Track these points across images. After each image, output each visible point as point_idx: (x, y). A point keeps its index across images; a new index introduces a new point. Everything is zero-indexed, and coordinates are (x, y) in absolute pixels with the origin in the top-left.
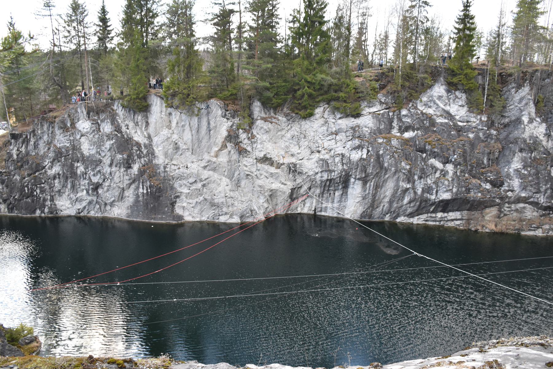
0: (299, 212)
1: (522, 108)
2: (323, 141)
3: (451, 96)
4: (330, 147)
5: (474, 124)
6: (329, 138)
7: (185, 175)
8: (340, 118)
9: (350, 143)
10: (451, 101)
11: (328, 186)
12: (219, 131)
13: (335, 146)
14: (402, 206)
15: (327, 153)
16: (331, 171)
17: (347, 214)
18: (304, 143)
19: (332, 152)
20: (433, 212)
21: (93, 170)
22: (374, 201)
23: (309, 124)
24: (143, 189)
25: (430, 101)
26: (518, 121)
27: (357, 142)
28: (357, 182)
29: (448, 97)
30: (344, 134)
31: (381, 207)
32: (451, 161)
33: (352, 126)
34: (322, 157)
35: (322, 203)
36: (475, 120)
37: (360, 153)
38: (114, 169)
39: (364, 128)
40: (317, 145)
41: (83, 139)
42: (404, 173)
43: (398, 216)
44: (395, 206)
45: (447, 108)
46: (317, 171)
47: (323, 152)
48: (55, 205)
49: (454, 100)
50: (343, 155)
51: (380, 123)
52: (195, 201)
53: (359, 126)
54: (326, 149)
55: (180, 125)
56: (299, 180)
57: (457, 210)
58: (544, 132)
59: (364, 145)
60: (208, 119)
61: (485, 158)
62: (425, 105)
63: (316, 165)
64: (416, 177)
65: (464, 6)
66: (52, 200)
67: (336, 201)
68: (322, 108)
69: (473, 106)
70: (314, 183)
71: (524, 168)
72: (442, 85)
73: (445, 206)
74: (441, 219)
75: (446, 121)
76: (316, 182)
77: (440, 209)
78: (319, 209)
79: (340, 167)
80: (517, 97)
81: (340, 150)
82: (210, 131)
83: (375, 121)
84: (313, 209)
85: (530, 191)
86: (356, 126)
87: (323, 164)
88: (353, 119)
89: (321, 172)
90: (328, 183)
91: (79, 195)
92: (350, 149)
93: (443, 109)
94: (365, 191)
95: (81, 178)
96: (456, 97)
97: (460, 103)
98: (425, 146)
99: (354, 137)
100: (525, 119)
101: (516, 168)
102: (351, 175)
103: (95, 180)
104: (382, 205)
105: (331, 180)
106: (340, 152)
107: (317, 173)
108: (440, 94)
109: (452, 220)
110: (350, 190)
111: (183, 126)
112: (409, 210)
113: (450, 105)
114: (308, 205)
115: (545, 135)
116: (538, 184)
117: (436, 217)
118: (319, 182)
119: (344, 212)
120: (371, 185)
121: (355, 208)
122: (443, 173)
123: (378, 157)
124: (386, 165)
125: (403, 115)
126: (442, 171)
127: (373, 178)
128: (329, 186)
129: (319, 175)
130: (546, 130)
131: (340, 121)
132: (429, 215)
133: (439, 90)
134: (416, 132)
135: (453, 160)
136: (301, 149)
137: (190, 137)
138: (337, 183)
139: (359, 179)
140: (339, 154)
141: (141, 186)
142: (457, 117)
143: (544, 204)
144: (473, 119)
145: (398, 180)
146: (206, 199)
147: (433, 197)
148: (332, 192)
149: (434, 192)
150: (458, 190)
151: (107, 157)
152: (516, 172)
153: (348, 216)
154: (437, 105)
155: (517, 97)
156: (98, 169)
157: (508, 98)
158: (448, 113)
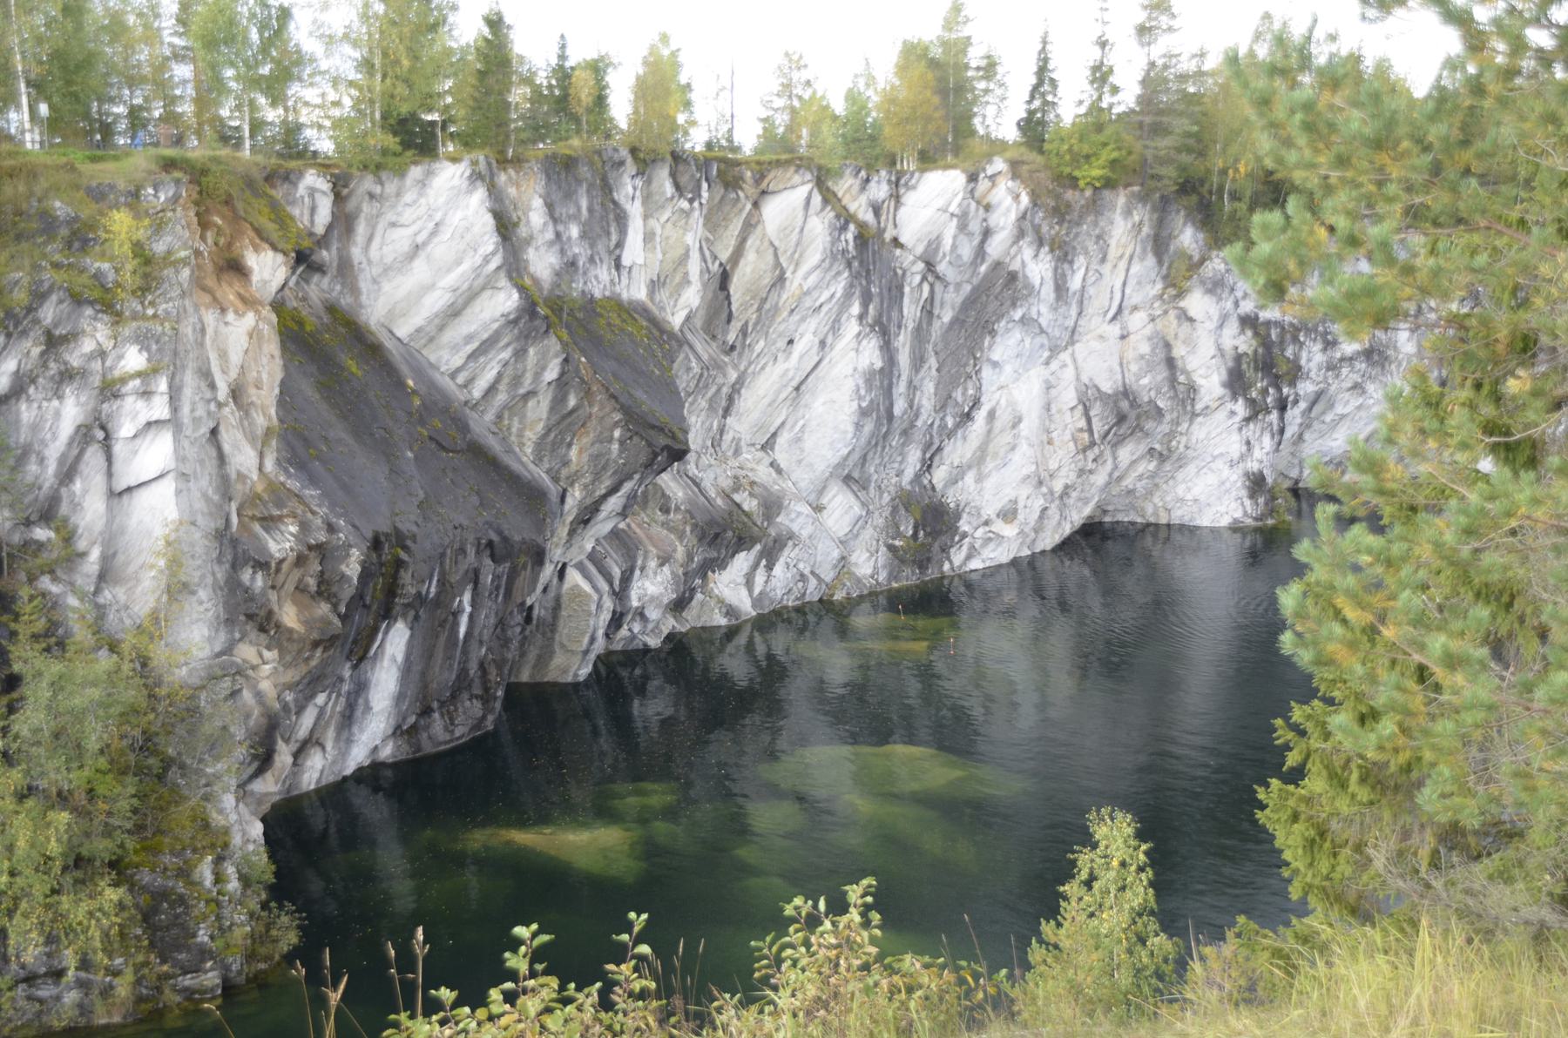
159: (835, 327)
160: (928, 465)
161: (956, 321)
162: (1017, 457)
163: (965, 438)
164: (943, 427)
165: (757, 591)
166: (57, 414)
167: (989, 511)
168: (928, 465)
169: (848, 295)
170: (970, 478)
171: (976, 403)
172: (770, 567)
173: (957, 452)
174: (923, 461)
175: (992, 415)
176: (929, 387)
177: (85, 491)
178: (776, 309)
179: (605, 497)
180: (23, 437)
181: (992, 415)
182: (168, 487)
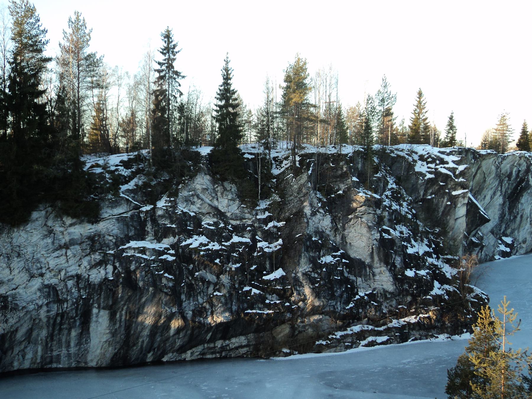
0: (15, 369)
1: (302, 199)
2: (48, 259)
3: (219, 188)
6: (56, 254)
8: (71, 225)
9: (88, 258)
10: (219, 194)
11: (57, 325)
13: (66, 265)
14: (168, 339)
15: (54, 276)
16: (60, 302)
17: (92, 360)
18: (17, 264)
19: (63, 273)
20: (209, 342)
23: (25, 236)
25: (193, 195)
26: (300, 213)
27: (97, 257)
28: (102, 312)
29: (214, 189)
30: (78, 247)
31: (140, 344)
32: (226, 271)
33: (89, 234)
34: (46, 282)
35: (52, 351)
37: (103, 272)
39: (107, 237)
40: (38, 265)
42: (166, 294)
44: (159, 339)
45: (216, 203)
46: (40, 303)
47: (48, 275)
49: (222, 194)
50: (78, 277)
51: (128, 228)
53: (99, 236)
54: (53, 270)
56: (12, 321)
57: (241, 334)
58: (330, 225)
59: (108, 260)
61: (267, 263)
62: (186, 201)
63: (39, 294)
64: (183, 297)
65: (224, 79)
67: (72, 344)
68: (43, 213)
70: (37, 321)
71: (313, 271)
72: (205, 174)
74: (223, 348)
76: (40, 320)
77: (219, 336)
78: (48, 360)
79: (76, 294)
81: (73, 270)
83: (122, 226)
84: (39, 361)
85: (324, 297)
86: (95, 236)
87: (49, 292)
88: (89, 226)
89: (47, 305)
90: (59, 319)
92: (88, 267)
93: (210, 205)
94: (115, 324)
96: (225, 189)
97: (230, 197)
98: (191, 255)
99: (93, 250)
100: (307, 211)
101: (304, 272)
102: (92, 304)
104: (141, 340)
105: (62, 315)
106: (74, 273)
107: (40, 307)
108: (204, 187)
109: (237, 348)
112: (179, 343)
113: (217, 199)
114: (29, 356)
115: (332, 228)
116: (331, 289)
117: (215, 347)
118: (45, 320)
119: (86, 358)
120: (122, 315)
121: (102, 351)
122: (218, 287)
123: (129, 273)
124: (141, 284)
125: (159, 216)
126: (215, 284)
127: (124, 305)
128: (61, 324)
129: (45, 308)
130: (332, 223)
131: (72, 230)
132: (206, 345)
133: (202, 181)
134: (177, 237)
135: (228, 269)
136: (13, 274)
138: (72, 318)
139: (104, 308)
140: (72, 276)
142: (229, 215)
143: (342, 312)
148: (65, 332)
149: (209, 313)
150: (239, 307)
152: (305, 276)
154: (202, 200)
157: (285, 187)
158: (216, 209)
159: (494, 194)
160: (506, 229)
161: (511, 193)
162: (527, 227)
163: (515, 222)
164: (510, 219)
165: (479, 258)
166: (443, 202)
167: (520, 240)
168: (506, 229)
169: (498, 185)
170: (516, 232)
171: (518, 214)
172: (481, 252)
173: (513, 226)
174: (505, 227)
175: (522, 217)
176: (507, 209)
177: (450, 219)
178: (483, 188)
179: (473, 231)
180: (434, 207)
181: (522, 217)
182: (464, 219)
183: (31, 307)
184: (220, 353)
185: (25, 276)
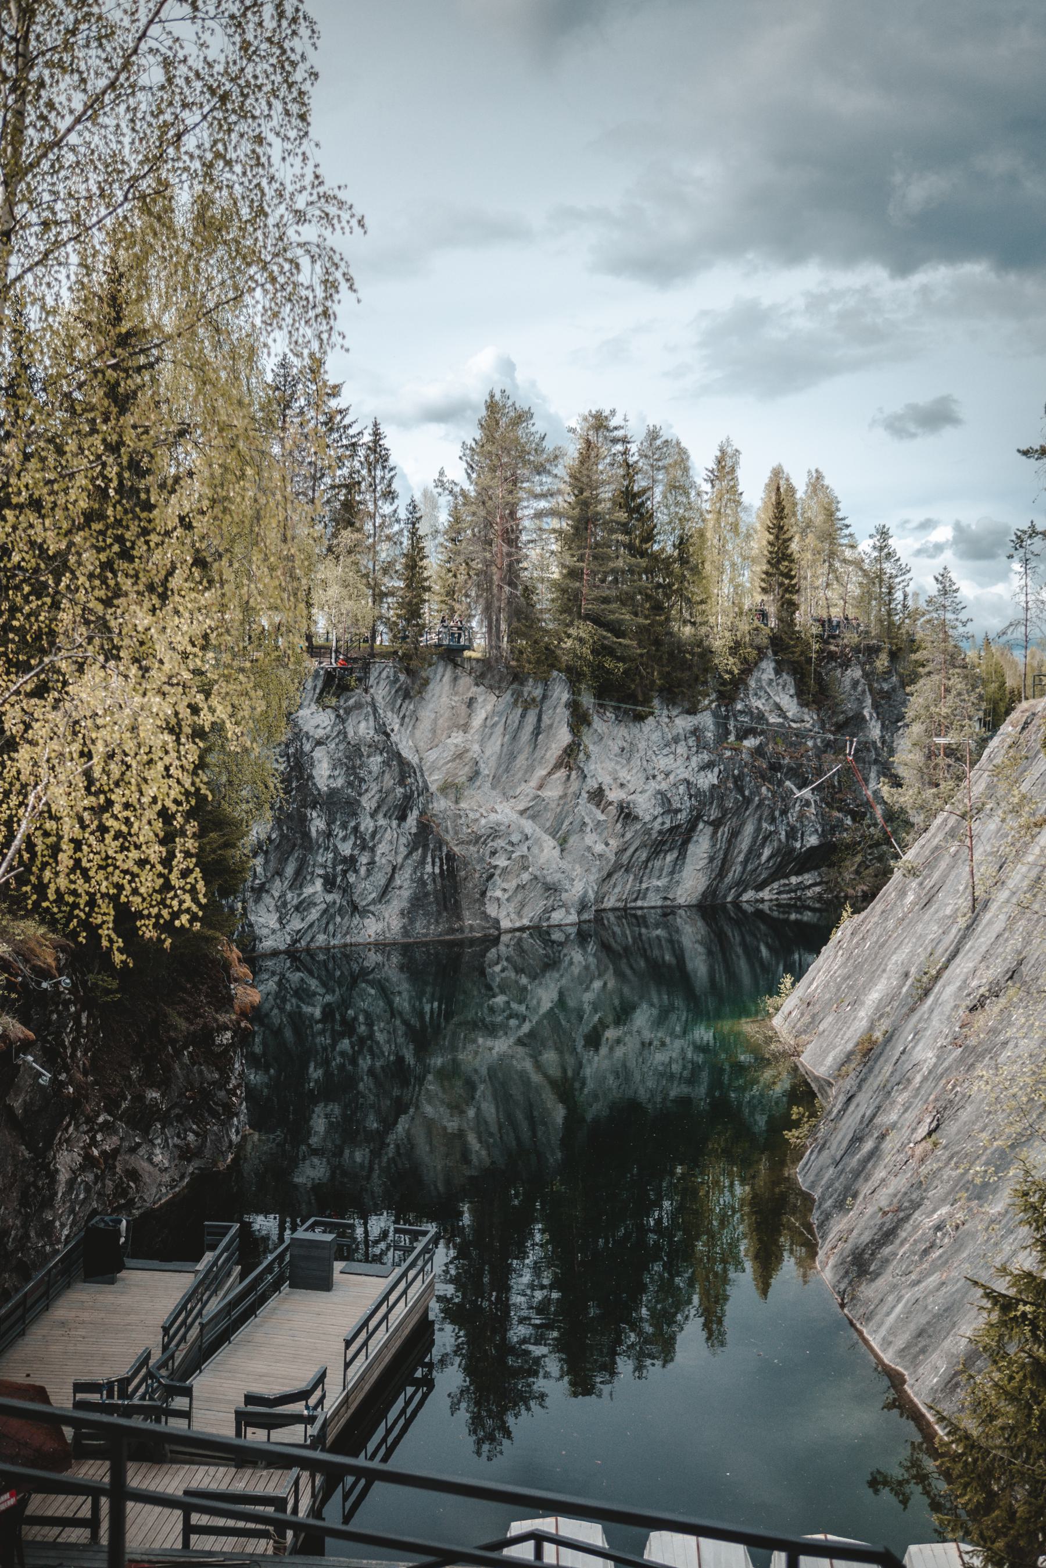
4: (669, 768)
5: (808, 726)
6: (665, 752)
7: (502, 828)
12: (554, 735)
19: (672, 777)
21: (344, 826)
22: (724, 861)
24: (433, 864)
27: (706, 757)
36: (810, 719)
38: (382, 822)
41: (319, 753)
43: (745, 891)
45: (778, 700)
47: (659, 778)
48: (251, 925)
49: (784, 687)
50: (688, 782)
52: (514, 884)
55: (489, 723)
56: (628, 835)
60: (541, 711)
63: (653, 801)
66: (245, 914)
69: (801, 695)
73: (808, 861)
75: (781, 720)
80: (847, 683)
82: (538, 734)
91: (308, 891)
95: (320, 847)
100: (866, 713)
103: (346, 849)
107: (656, 818)
110: (691, 847)
111: (495, 725)
120: (724, 831)
129: (659, 820)
132: (782, 882)
137: (497, 748)
141: (429, 860)
142: (790, 714)
144: (807, 718)
145: (760, 819)
146: (536, 878)
147: (798, 845)
151: (369, 795)
153: (681, 901)
155: (847, 683)
156: (353, 824)
183: (647, 818)
184: (795, 891)
185: (642, 776)
